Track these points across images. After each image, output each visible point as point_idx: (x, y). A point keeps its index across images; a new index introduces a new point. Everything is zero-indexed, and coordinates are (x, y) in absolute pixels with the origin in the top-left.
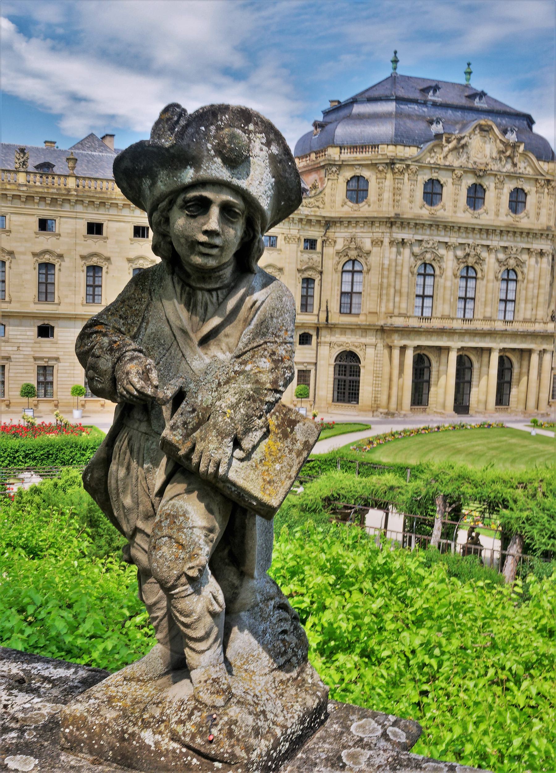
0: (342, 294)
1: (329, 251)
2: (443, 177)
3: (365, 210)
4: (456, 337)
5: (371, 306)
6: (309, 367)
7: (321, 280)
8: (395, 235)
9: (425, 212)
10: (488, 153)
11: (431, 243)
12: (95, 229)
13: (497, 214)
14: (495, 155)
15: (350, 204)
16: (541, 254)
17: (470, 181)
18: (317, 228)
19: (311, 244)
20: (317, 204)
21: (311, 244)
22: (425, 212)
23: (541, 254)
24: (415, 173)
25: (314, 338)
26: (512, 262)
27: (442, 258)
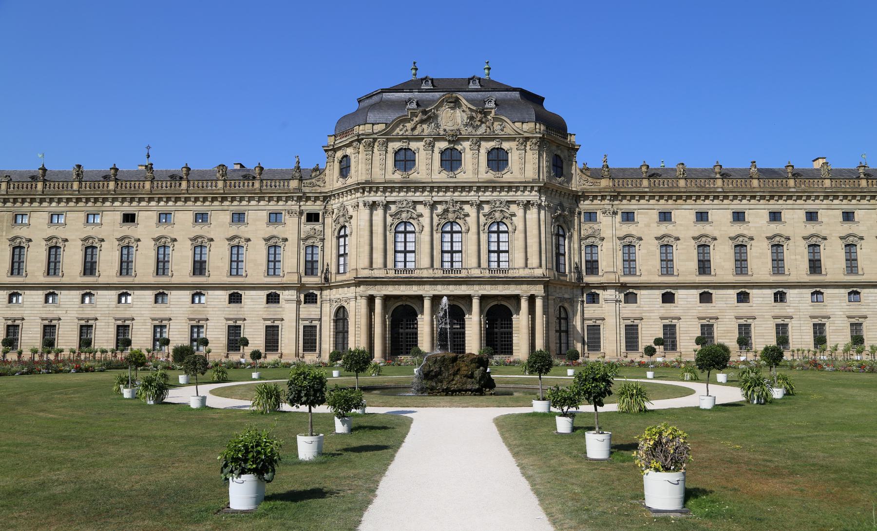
0: (339, 256)
1: (329, 221)
2: (413, 145)
3: (350, 181)
4: (427, 287)
5: (357, 262)
6: (314, 323)
7: (323, 246)
8: (366, 199)
9: (398, 176)
11: (405, 203)
12: (129, 218)
14: (466, 120)
15: (341, 179)
16: (527, 205)
17: (443, 145)
18: (318, 203)
19: (313, 217)
20: (318, 183)
21: (313, 217)
22: (398, 176)
23: (527, 205)
24: (385, 144)
25: (319, 297)
26: (498, 215)
27: (421, 215)
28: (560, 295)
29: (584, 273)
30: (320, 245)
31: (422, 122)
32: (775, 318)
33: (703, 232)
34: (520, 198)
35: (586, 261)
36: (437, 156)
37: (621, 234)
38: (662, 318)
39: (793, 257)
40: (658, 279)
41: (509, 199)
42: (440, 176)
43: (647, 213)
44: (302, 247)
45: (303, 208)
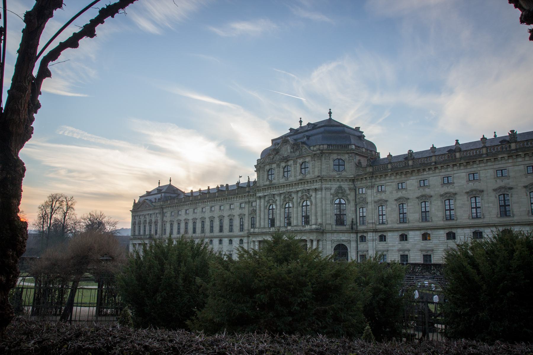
10: (289, 151)
13: (295, 177)
16: (316, 190)
17: (283, 164)
24: (264, 168)
28: (338, 238)
29: (358, 225)
30: (255, 216)
31: (276, 154)
33: (424, 193)
34: (313, 187)
35: (360, 217)
36: (282, 170)
37: (376, 199)
38: (399, 250)
39: (486, 205)
40: (396, 226)
41: (308, 188)
42: (282, 181)
43: (391, 185)
44: (250, 218)
45: (250, 200)
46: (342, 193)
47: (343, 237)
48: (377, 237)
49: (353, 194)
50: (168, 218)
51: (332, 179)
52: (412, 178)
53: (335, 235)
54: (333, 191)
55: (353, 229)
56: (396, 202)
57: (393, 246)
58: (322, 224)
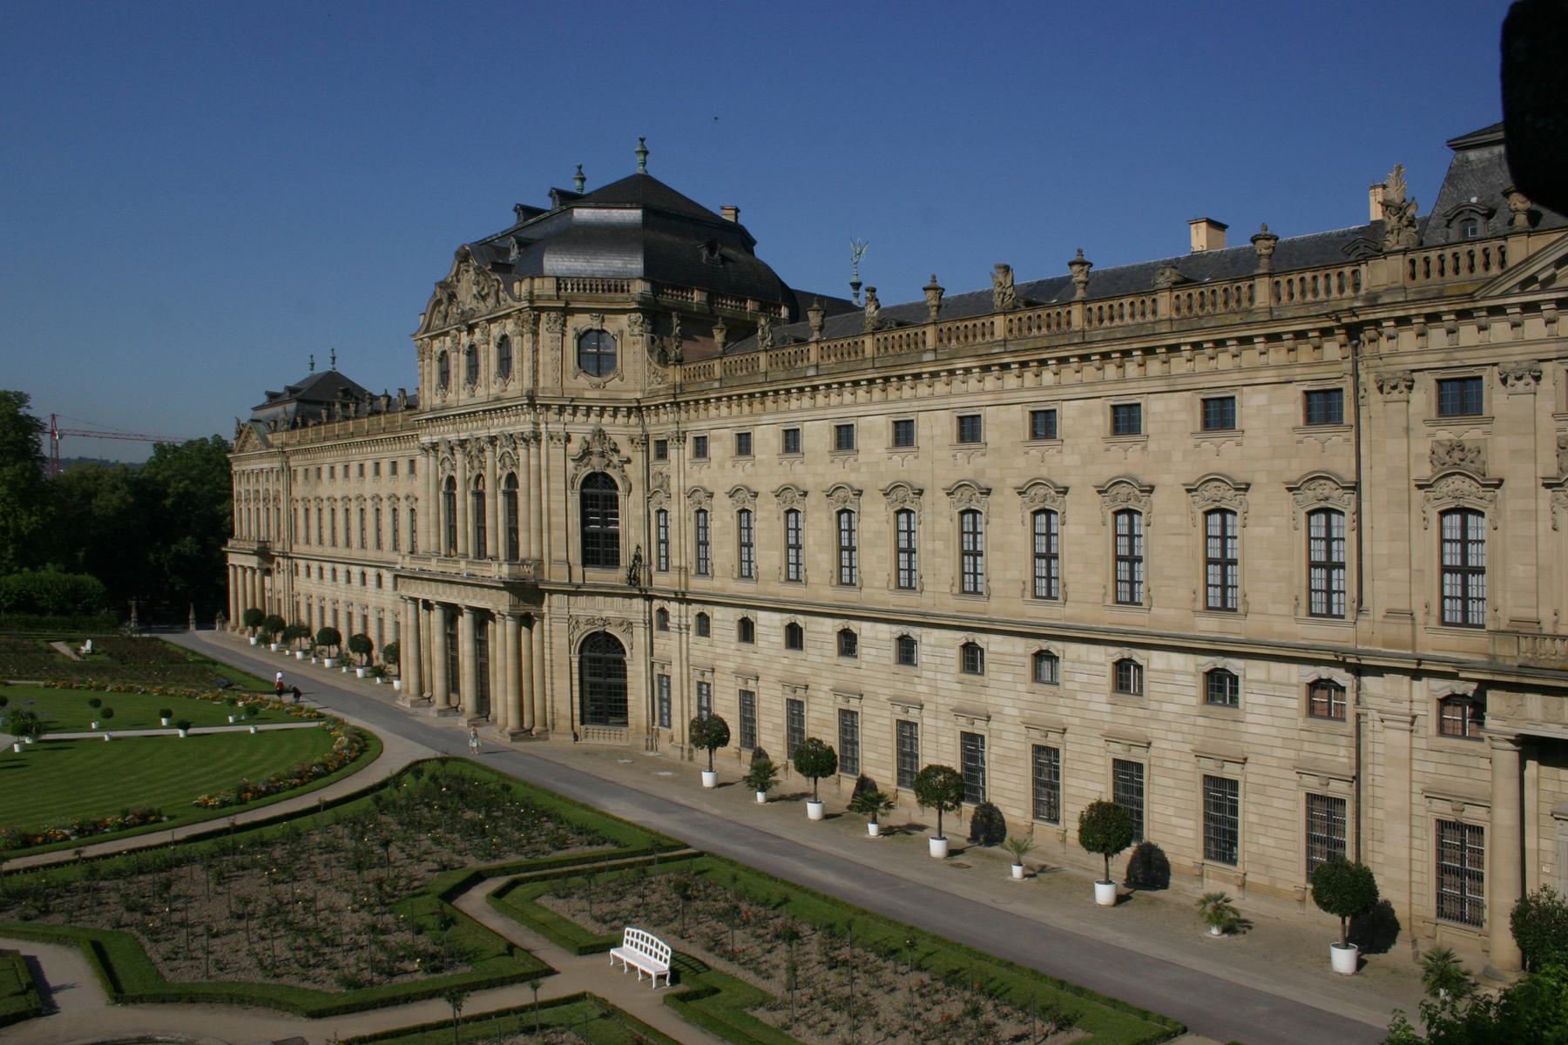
28: (590, 613)
29: (654, 569)
32: (894, 701)
37: (690, 483)
46: (602, 455)
47: (609, 610)
48: (692, 621)
49: (638, 458)
50: (299, 490)
51: (570, 406)
52: (766, 419)
53: (582, 600)
54: (575, 447)
55: (635, 587)
56: (730, 501)
57: (725, 657)
58: (541, 561)
